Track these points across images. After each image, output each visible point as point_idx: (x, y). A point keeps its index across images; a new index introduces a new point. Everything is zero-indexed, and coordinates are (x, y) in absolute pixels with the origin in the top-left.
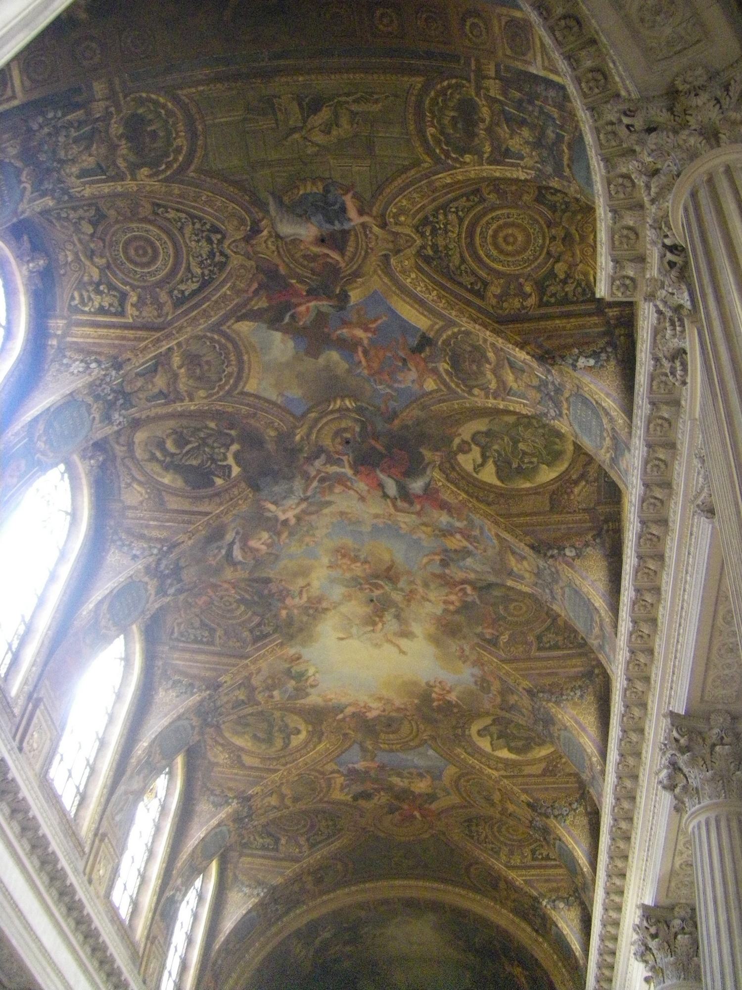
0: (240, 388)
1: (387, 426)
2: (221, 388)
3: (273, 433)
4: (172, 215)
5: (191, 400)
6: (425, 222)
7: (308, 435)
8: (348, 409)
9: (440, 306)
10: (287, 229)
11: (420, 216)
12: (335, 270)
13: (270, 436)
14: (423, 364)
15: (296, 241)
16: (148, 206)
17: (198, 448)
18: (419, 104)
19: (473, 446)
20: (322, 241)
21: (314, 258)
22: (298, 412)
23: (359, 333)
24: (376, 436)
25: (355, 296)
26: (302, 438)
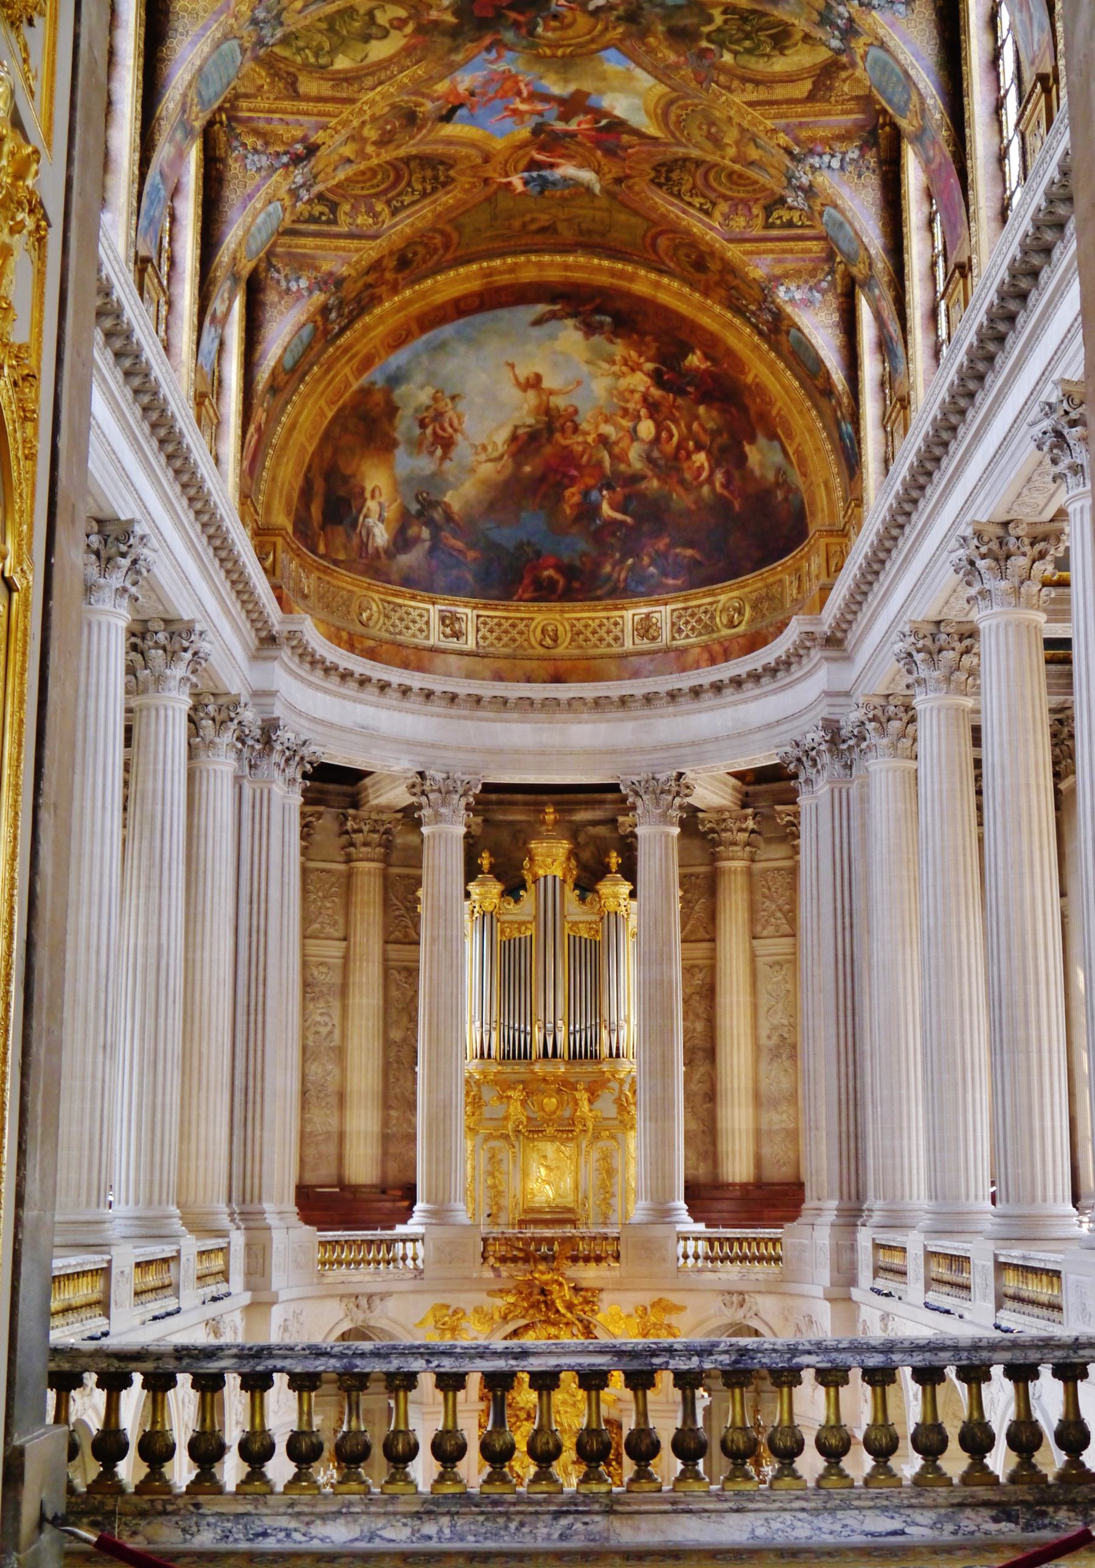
0: (674, 95)
1: (499, 37)
2: (696, 105)
3: (651, 40)
4: (697, 201)
5: (730, 119)
6: (444, 185)
7: (606, 29)
8: (549, 46)
9: (428, 149)
10: (587, 176)
11: (449, 188)
12: (542, 148)
13: (656, 37)
14: (451, 99)
15: (581, 167)
16: (717, 214)
17: (761, 29)
18: (447, 247)
19: (387, 25)
20: (552, 166)
21: (561, 156)
22: (611, 53)
23: (524, 107)
24: (517, 25)
25: (524, 133)
26: (614, 28)
